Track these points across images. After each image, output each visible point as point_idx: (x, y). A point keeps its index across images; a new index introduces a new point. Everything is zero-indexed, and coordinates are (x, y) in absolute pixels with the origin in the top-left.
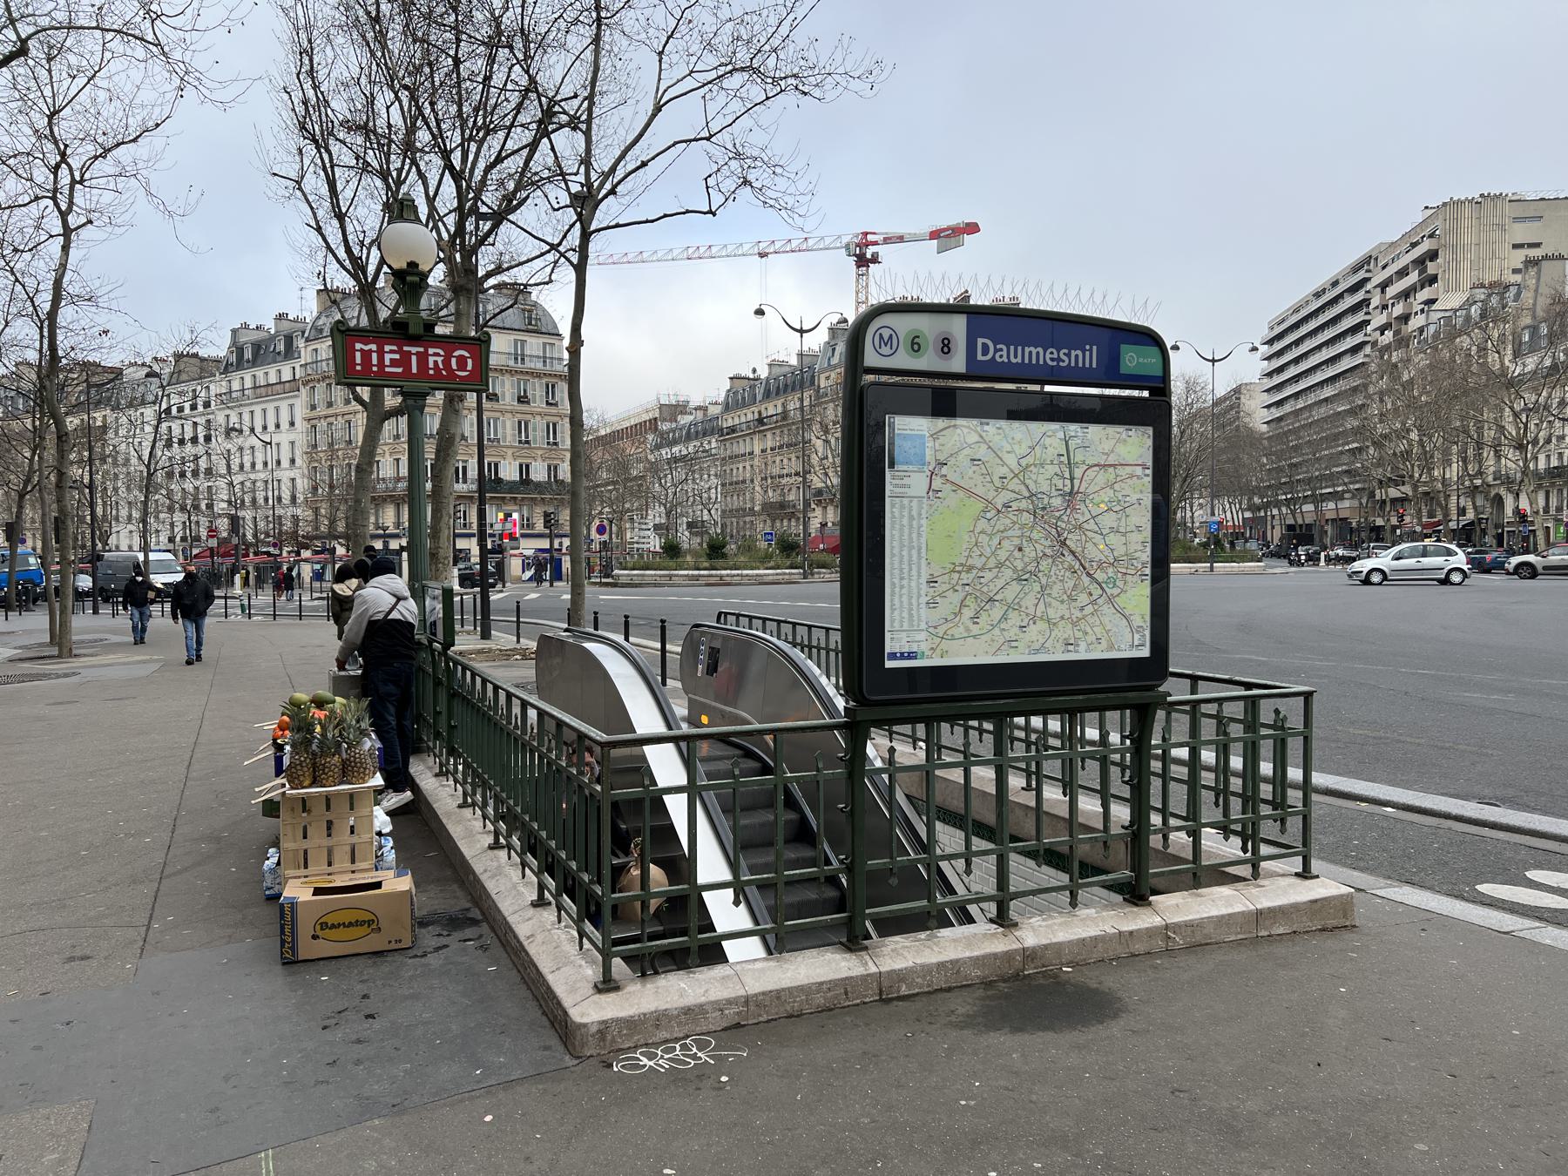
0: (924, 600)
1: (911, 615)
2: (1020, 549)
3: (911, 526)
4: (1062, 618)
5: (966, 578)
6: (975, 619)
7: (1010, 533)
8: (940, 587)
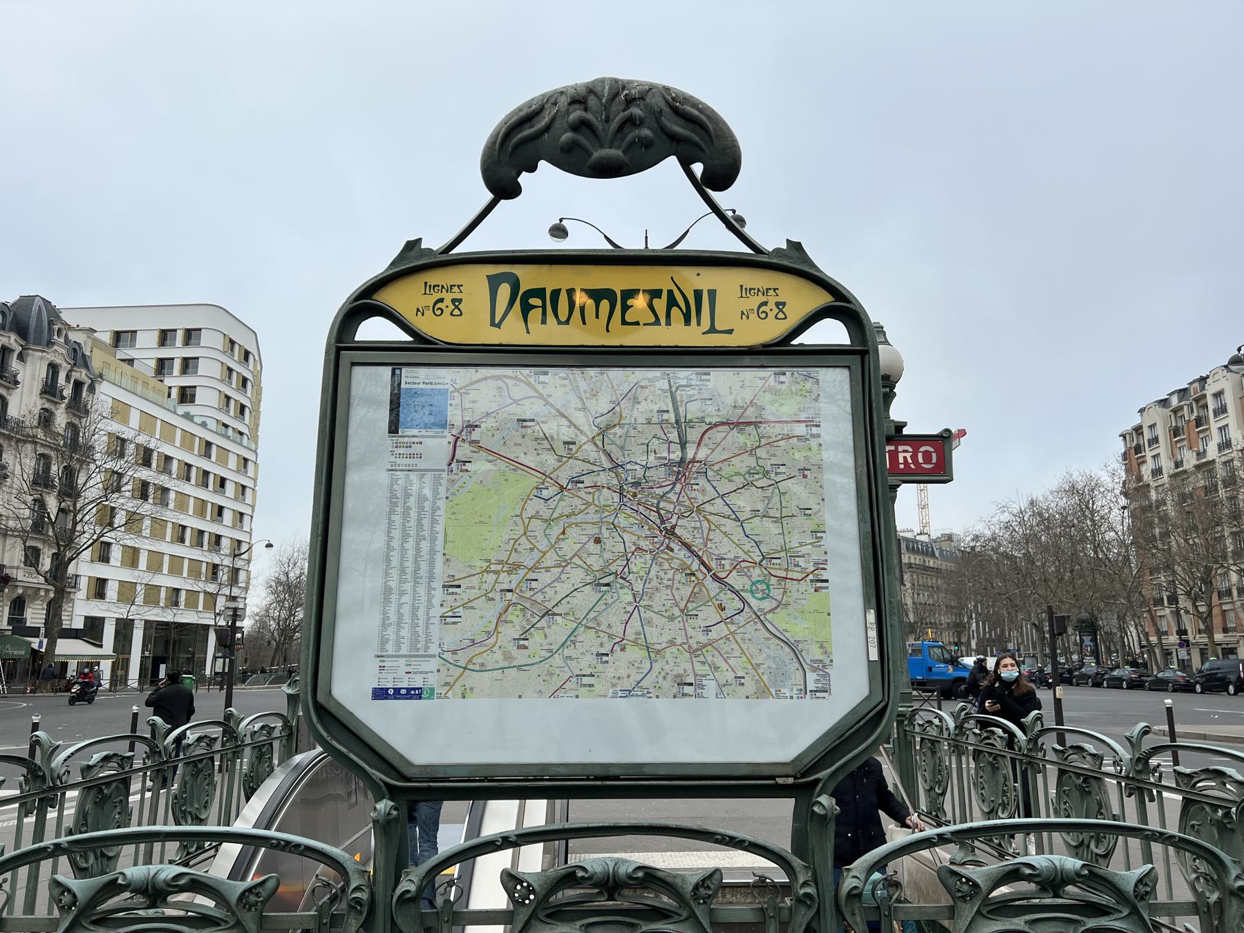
0: (437, 611)
1: (415, 635)
2: (598, 541)
3: (421, 509)
4: (672, 643)
5: (506, 580)
6: (521, 642)
7: (580, 518)
8: (464, 594)
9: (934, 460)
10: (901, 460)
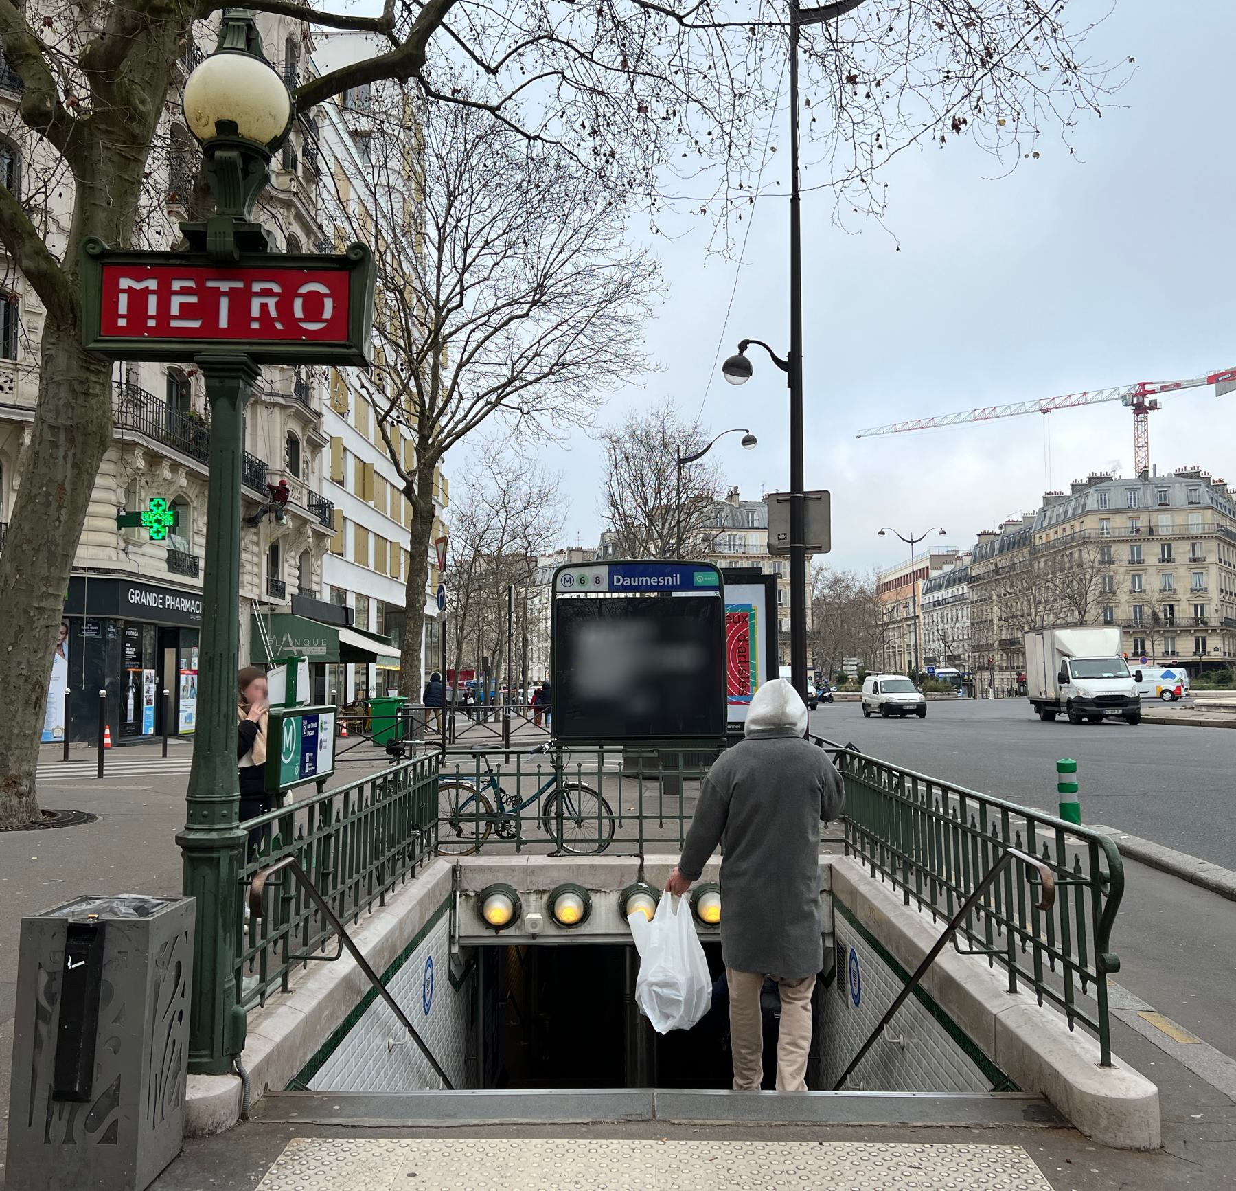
9: (327, 314)
10: (255, 312)
